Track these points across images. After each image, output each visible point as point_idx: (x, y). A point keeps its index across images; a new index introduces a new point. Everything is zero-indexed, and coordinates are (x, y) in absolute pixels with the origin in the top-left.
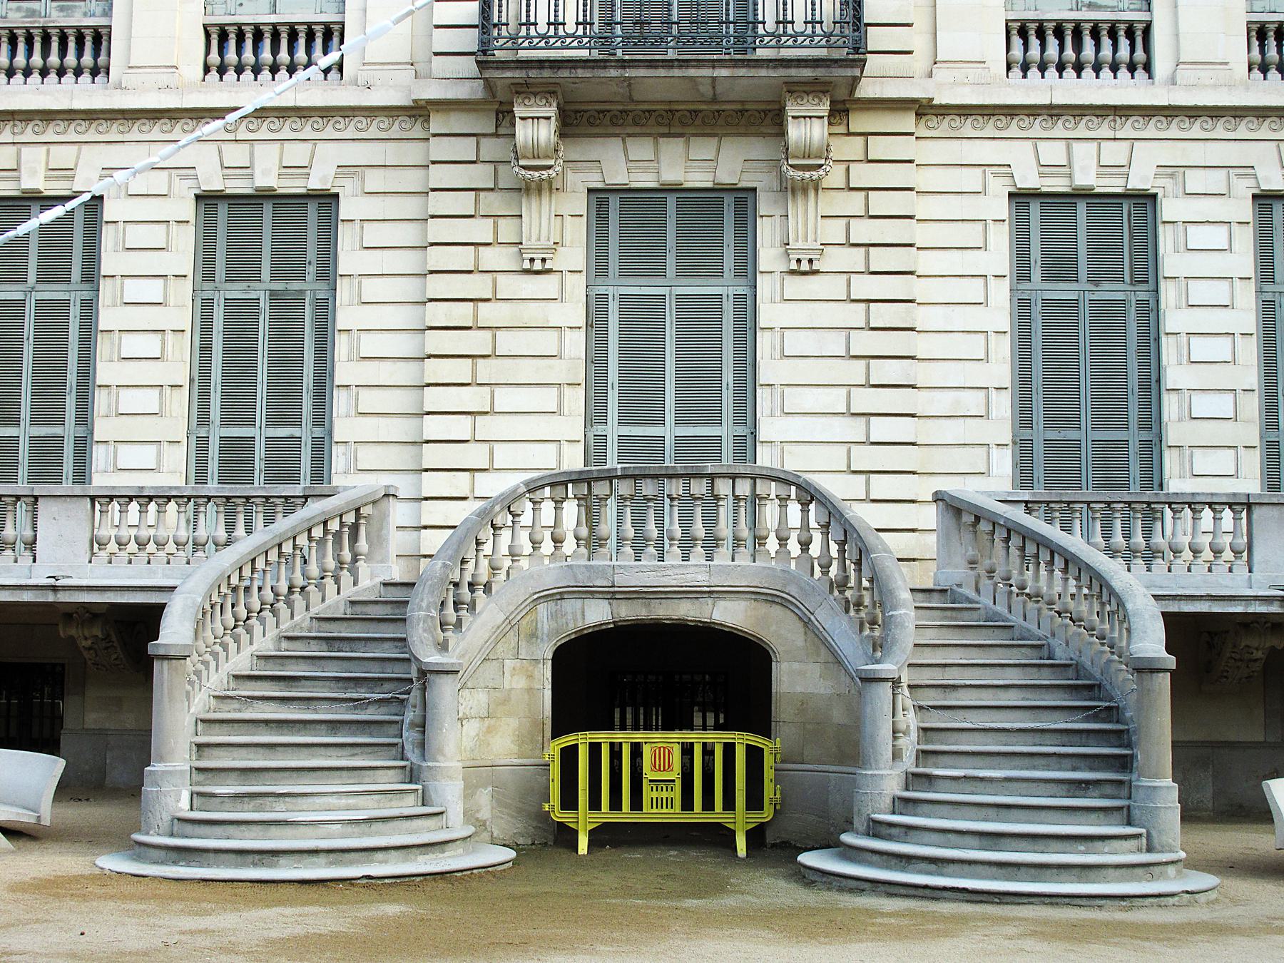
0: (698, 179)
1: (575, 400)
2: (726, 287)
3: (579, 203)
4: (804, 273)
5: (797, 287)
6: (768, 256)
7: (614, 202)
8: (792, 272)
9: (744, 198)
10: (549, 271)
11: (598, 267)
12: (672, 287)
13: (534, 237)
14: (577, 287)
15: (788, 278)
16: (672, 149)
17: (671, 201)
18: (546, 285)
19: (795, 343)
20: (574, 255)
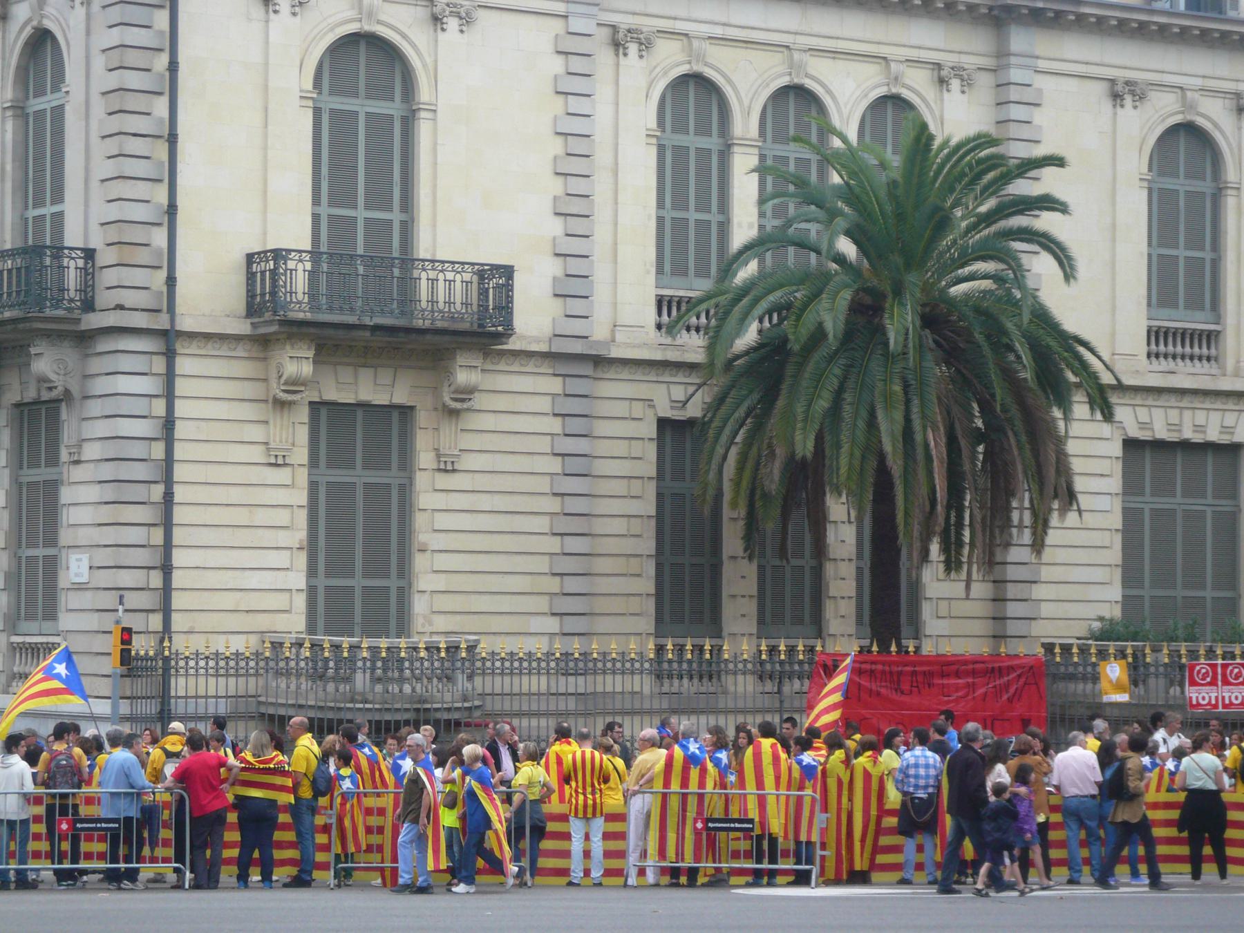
0: (381, 399)
1: (302, 560)
2: (391, 477)
3: (303, 414)
4: (446, 471)
5: (443, 481)
6: (425, 459)
7: (324, 412)
8: (439, 470)
9: (406, 412)
10: (285, 465)
11: (313, 462)
12: (359, 476)
13: (278, 439)
14: (303, 476)
15: (437, 475)
16: (366, 375)
17: (360, 414)
18: (283, 475)
19: (442, 521)
20: (301, 455)
